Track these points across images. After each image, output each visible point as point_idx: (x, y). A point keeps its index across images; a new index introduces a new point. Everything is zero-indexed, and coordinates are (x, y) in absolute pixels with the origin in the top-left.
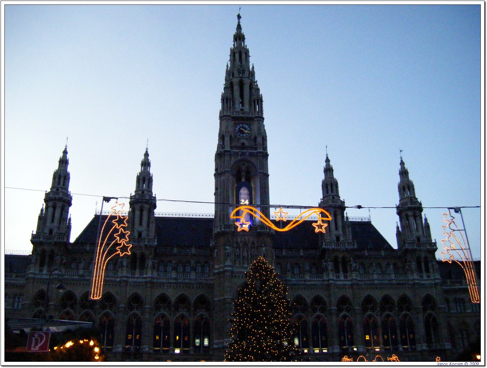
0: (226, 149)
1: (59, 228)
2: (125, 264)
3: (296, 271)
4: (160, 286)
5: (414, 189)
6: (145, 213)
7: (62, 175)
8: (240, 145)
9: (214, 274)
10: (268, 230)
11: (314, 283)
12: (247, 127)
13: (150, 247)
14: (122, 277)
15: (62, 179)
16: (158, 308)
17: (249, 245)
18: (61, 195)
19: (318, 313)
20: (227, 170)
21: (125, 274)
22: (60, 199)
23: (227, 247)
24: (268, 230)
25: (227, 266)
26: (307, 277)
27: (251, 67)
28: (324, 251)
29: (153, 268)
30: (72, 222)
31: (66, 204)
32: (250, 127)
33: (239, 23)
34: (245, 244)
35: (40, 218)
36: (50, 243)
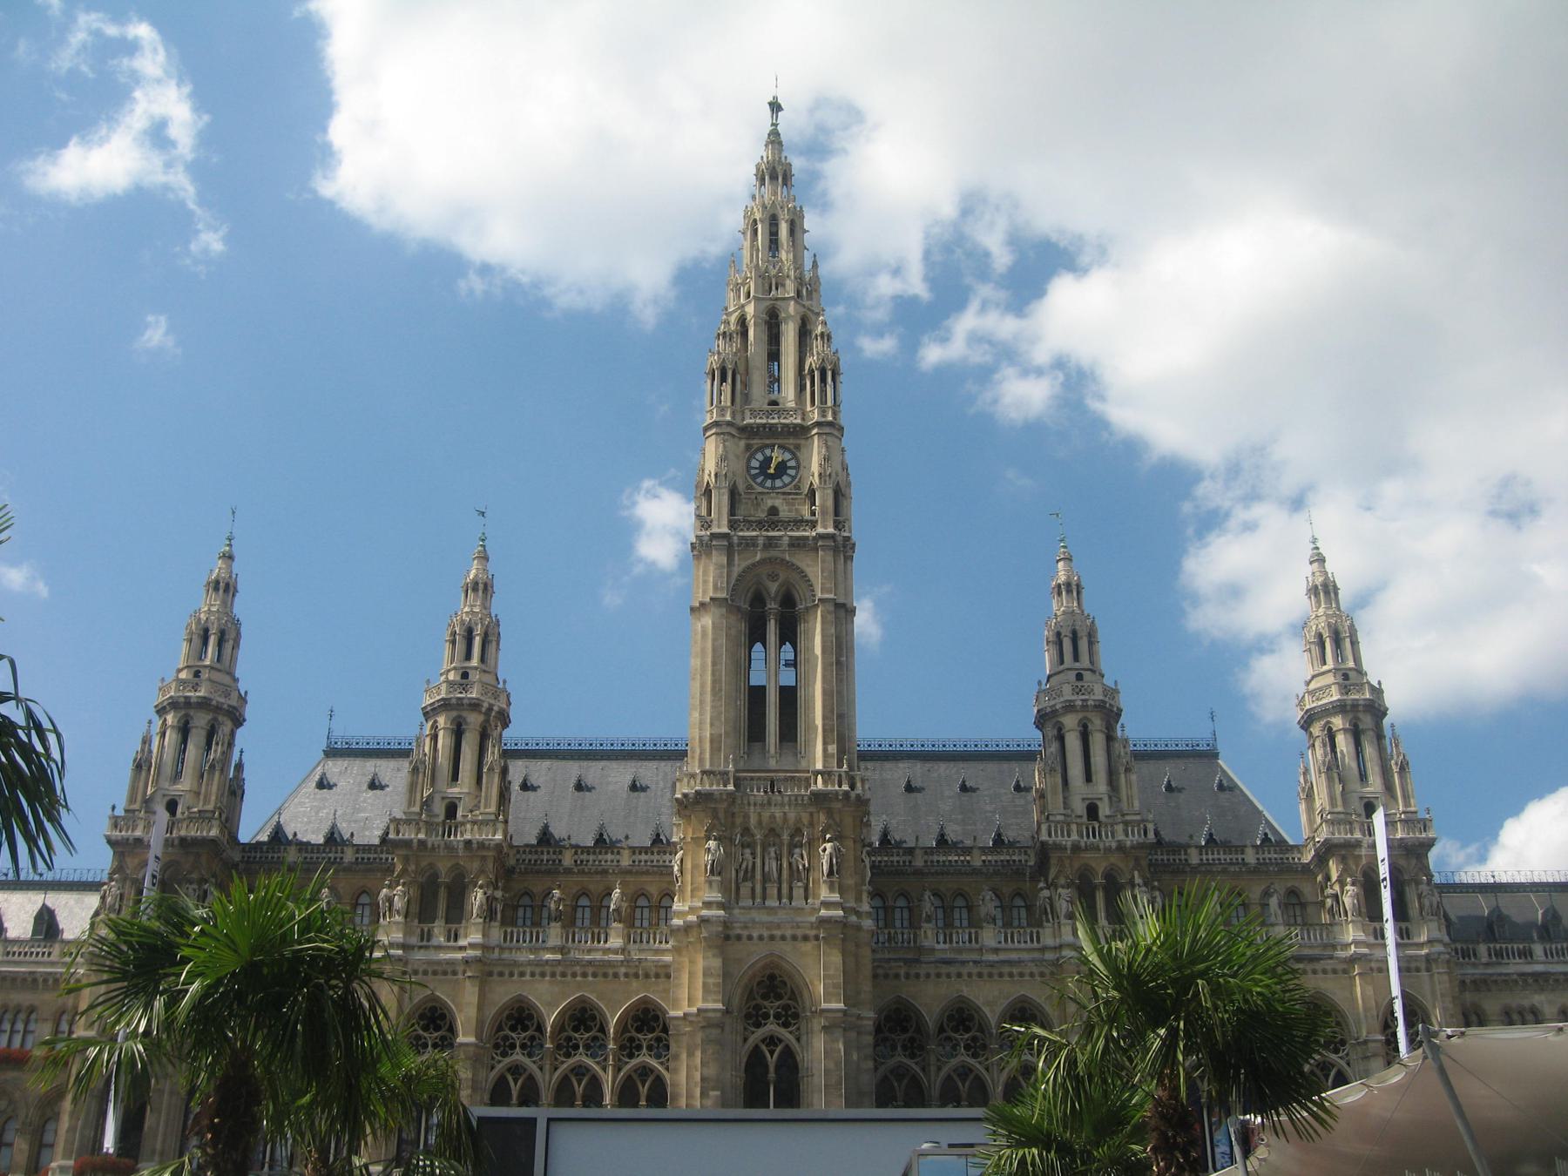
0: (715, 530)
2: (398, 903)
4: (511, 975)
5: (1355, 643)
7: (213, 630)
9: (675, 931)
10: (845, 787)
11: (1014, 956)
12: (787, 456)
13: (482, 845)
14: (392, 945)
15: (212, 640)
16: (505, 1047)
17: (786, 837)
20: (719, 595)
21: (398, 936)
22: (204, 704)
23: (712, 844)
24: (845, 787)
25: (708, 905)
26: (989, 937)
27: (808, 264)
29: (489, 913)
31: (220, 718)
32: (795, 457)
33: (775, 125)
34: (772, 831)
35: (138, 767)
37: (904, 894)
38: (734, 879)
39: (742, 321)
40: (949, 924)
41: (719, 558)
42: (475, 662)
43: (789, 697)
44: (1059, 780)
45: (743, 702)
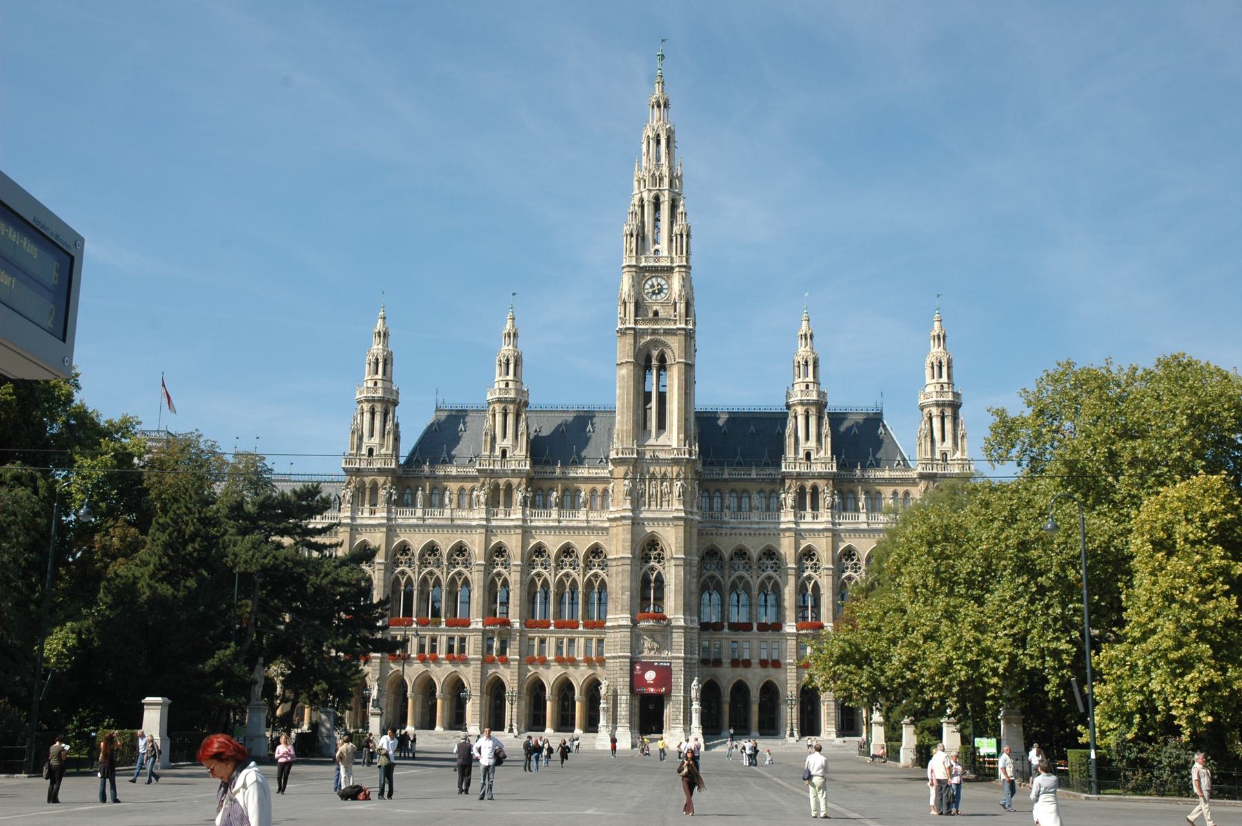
1: (382, 446)
3: (745, 501)
6: (510, 418)
7: (381, 360)
8: (651, 315)
9: (610, 520)
12: (663, 282)
15: (381, 366)
18: (380, 394)
19: (770, 572)
22: (381, 400)
23: (627, 482)
28: (785, 477)
29: (524, 504)
30: (400, 429)
36: (370, 472)
37: (718, 490)
38: (637, 499)
39: (642, 200)
40: (740, 508)
41: (629, 340)
42: (511, 377)
43: (662, 398)
44: (793, 440)
45: (641, 412)
